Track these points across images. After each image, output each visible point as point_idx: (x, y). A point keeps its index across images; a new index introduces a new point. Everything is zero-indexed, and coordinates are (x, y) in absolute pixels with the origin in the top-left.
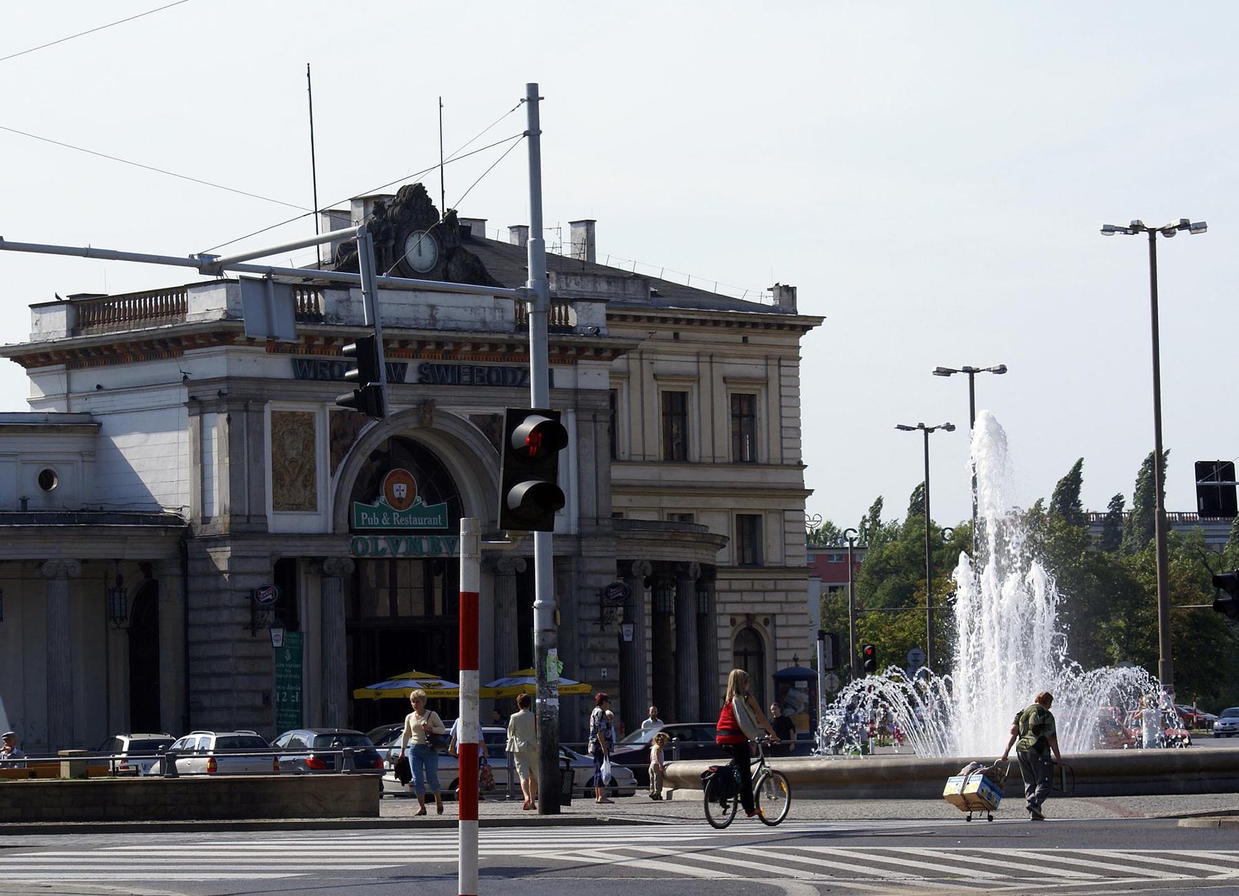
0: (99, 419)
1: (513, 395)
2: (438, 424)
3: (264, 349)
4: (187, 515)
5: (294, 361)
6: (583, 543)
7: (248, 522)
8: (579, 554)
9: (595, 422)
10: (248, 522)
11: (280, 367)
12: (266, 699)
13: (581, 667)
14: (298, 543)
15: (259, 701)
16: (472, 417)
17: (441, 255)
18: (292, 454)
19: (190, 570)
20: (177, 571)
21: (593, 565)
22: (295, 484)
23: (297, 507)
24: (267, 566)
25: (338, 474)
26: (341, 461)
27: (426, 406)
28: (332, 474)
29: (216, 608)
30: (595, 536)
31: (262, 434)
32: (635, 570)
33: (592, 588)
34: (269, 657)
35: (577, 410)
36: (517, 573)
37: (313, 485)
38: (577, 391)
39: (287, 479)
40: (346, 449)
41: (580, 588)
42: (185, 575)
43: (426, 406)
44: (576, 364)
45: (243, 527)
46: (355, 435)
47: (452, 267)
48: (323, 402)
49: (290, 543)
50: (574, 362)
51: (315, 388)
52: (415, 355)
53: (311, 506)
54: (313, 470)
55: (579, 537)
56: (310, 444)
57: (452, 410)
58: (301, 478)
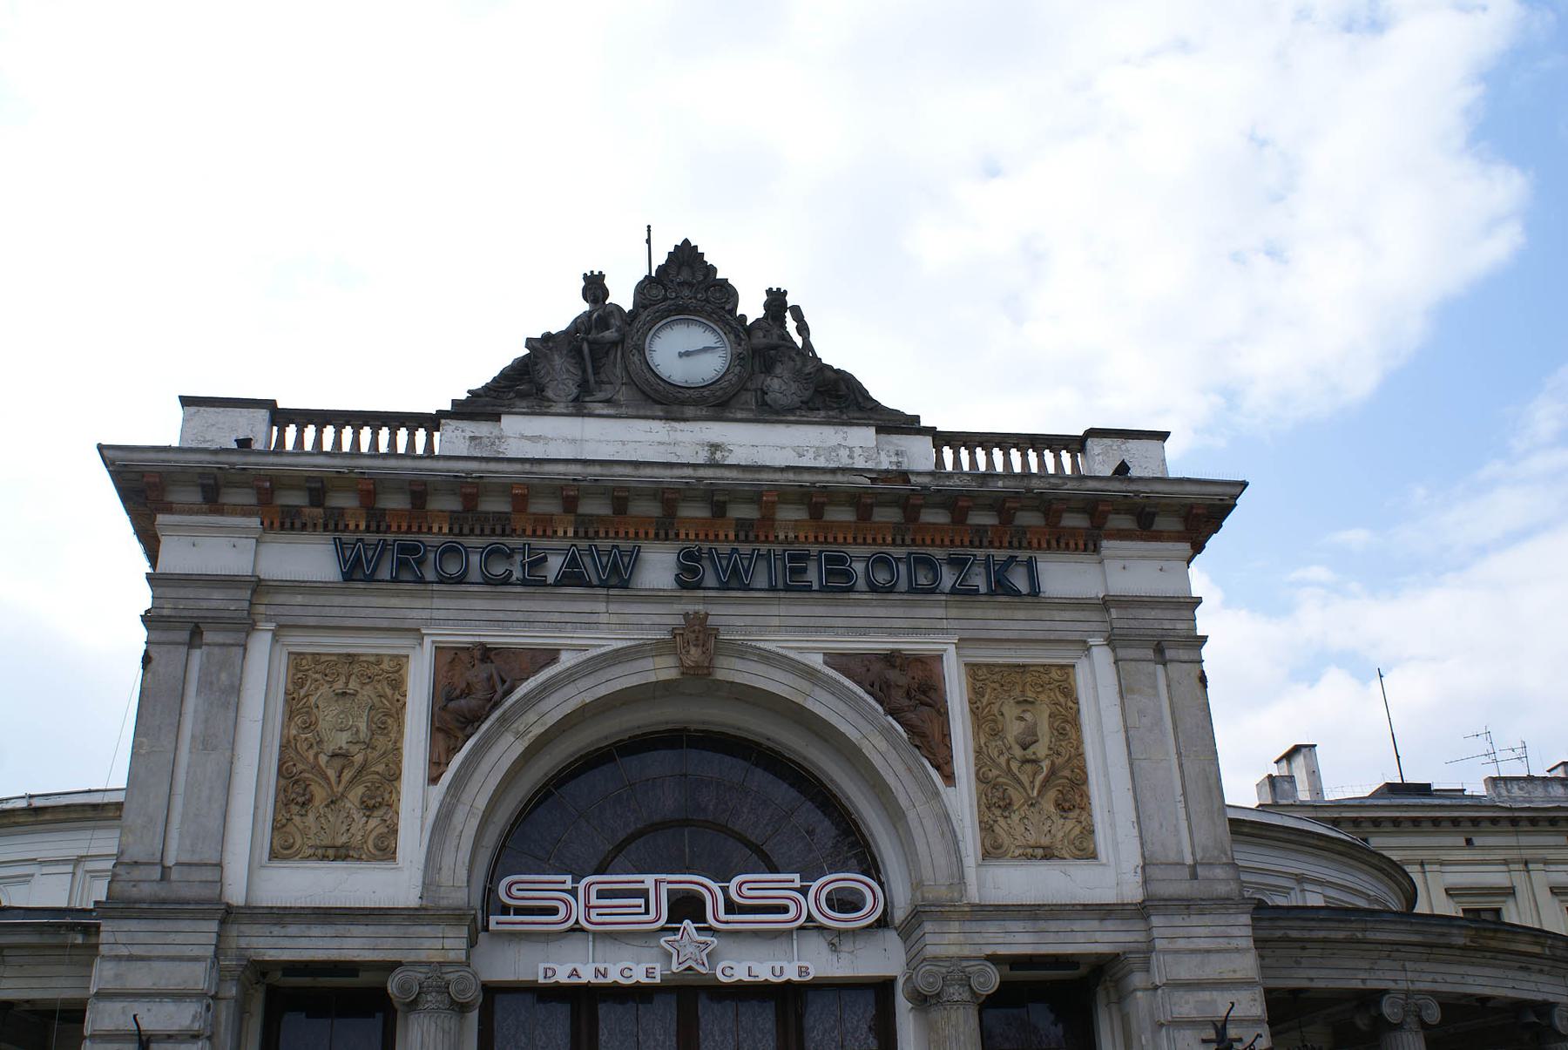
1: (940, 613)
2: (734, 671)
3: (255, 522)
5: (340, 546)
8: (1149, 950)
9: (1165, 664)
11: (308, 559)
14: (316, 930)
16: (838, 660)
17: (738, 359)
21: (1185, 970)
22: (327, 795)
23: (341, 853)
25: (447, 778)
27: (698, 633)
28: (434, 780)
30: (1187, 905)
32: (1388, 1010)
33: (1191, 1023)
35: (1112, 642)
40: (470, 721)
43: (698, 633)
44: (1096, 549)
45: (147, 890)
47: (775, 384)
50: (1088, 543)
51: (394, 602)
52: (664, 530)
55: (1142, 910)
56: (390, 716)
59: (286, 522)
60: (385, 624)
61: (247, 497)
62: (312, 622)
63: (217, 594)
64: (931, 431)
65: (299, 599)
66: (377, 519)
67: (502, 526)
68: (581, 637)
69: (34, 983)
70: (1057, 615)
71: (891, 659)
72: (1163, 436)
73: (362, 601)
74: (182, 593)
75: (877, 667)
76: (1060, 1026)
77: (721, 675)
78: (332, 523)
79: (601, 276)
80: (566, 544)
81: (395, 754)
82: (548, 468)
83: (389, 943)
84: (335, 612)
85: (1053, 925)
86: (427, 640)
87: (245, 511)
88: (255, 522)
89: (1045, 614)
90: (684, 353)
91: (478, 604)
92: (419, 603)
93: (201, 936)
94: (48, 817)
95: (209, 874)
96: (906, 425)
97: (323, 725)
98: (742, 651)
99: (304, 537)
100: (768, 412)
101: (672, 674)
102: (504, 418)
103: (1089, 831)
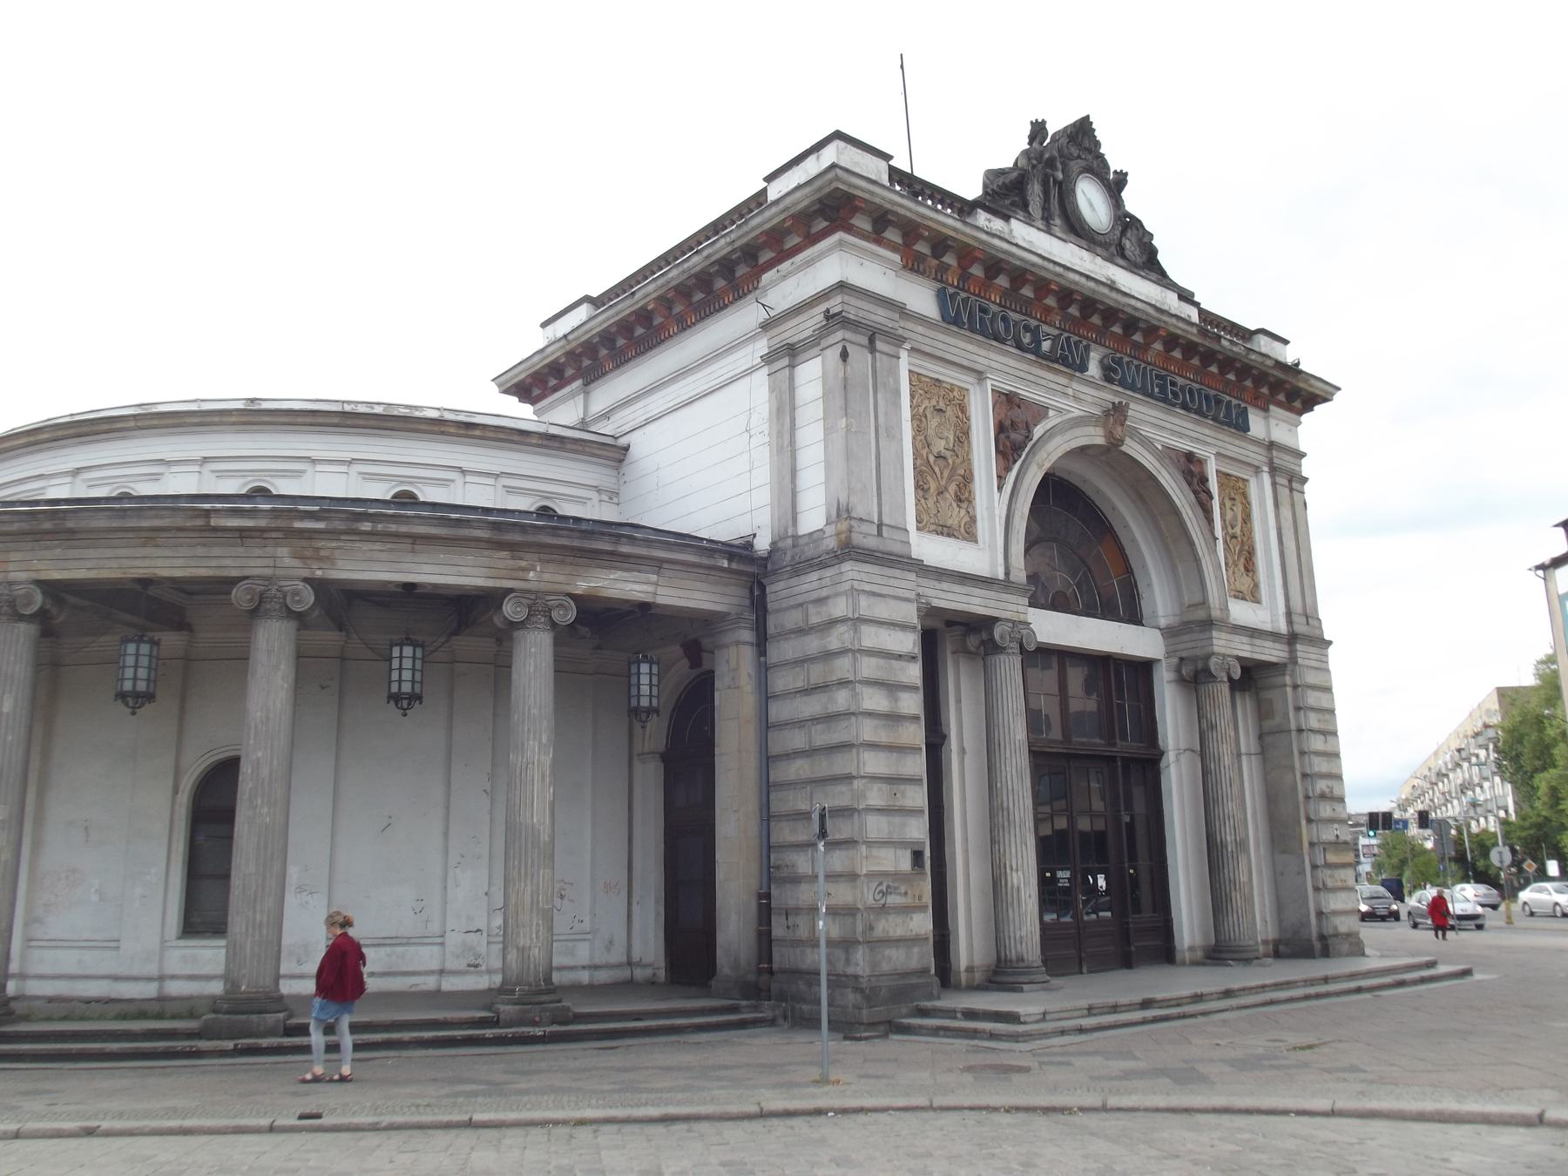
0: (623, 441)
4: (762, 544)
6: (1299, 647)
7: (880, 534)
8: (1293, 660)
10: (880, 534)
12: (917, 856)
13: (1309, 821)
14: (957, 588)
15: (905, 863)
18: (939, 446)
19: (771, 630)
20: (747, 635)
24: (910, 613)
26: (1008, 469)
28: (1000, 488)
29: (824, 688)
31: (897, 393)
34: (917, 781)
35: (1274, 470)
36: (1230, 679)
37: (970, 501)
38: (1272, 445)
39: (933, 486)
40: (1017, 449)
41: (1298, 709)
42: (762, 642)
43: (1117, 413)
46: (1028, 437)
47: (1127, 244)
48: (980, 376)
49: (945, 586)
51: (970, 347)
53: (968, 533)
54: (967, 479)
57: (1147, 431)
58: (952, 488)
59: (913, 265)
60: (965, 363)
61: (892, 235)
62: (927, 349)
63: (881, 311)
64: (1197, 305)
65: (920, 329)
66: (965, 276)
67: (1025, 307)
68: (1061, 402)
69: (681, 593)
70: (1251, 447)
71: (1190, 457)
72: (1286, 342)
73: (952, 341)
74: (860, 304)
75: (1183, 460)
76: (1094, 696)
77: (1124, 448)
78: (939, 275)
79: (1044, 122)
80: (1056, 332)
81: (967, 461)
82: (1071, 276)
83: (992, 604)
84: (941, 346)
85: (1258, 642)
86: (989, 382)
87: (893, 247)
88: (897, 258)
89: (1244, 444)
90: (1090, 200)
91: (1012, 363)
92: (983, 352)
93: (907, 583)
94: (478, 433)
95: (898, 536)
96: (1186, 297)
97: (931, 432)
98: (1135, 434)
99: (920, 279)
100: (1133, 267)
101: (1100, 441)
102: (1013, 221)
103: (1256, 586)
